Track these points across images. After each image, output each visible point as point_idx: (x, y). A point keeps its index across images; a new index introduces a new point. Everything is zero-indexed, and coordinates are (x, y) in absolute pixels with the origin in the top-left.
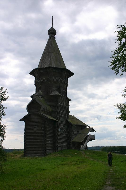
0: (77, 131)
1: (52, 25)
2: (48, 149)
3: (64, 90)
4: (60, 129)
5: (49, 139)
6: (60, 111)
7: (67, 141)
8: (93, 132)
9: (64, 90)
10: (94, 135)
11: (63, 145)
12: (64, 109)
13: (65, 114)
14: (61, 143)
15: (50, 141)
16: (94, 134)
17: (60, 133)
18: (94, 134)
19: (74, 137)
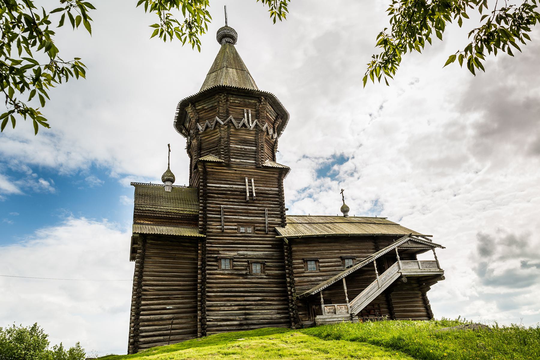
0: (341, 257)
1: (226, 23)
2: (158, 332)
3: (239, 146)
4: (225, 265)
5: (168, 299)
6: (220, 208)
7: (282, 298)
8: (431, 250)
9: (239, 146)
10: (437, 262)
11: (246, 314)
12: (248, 199)
13: (264, 214)
14: (236, 308)
15: (168, 307)
16: (436, 257)
17: (231, 274)
18: (436, 257)
19: (319, 278)
